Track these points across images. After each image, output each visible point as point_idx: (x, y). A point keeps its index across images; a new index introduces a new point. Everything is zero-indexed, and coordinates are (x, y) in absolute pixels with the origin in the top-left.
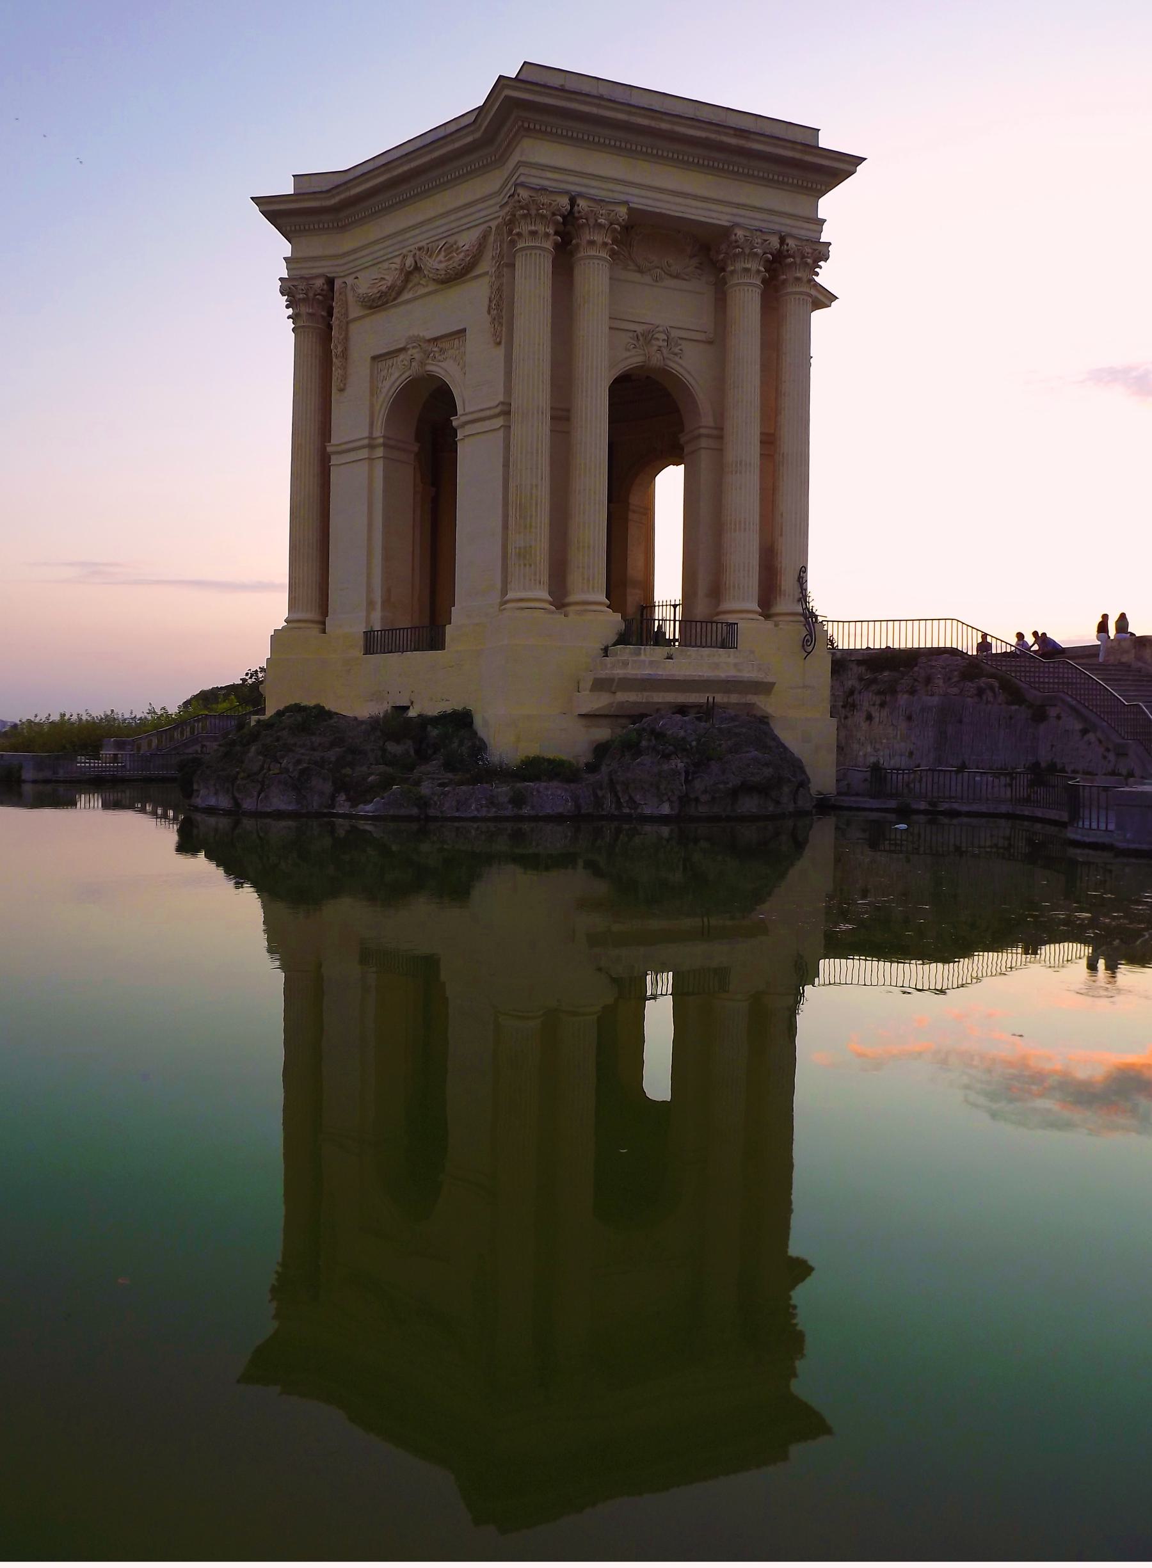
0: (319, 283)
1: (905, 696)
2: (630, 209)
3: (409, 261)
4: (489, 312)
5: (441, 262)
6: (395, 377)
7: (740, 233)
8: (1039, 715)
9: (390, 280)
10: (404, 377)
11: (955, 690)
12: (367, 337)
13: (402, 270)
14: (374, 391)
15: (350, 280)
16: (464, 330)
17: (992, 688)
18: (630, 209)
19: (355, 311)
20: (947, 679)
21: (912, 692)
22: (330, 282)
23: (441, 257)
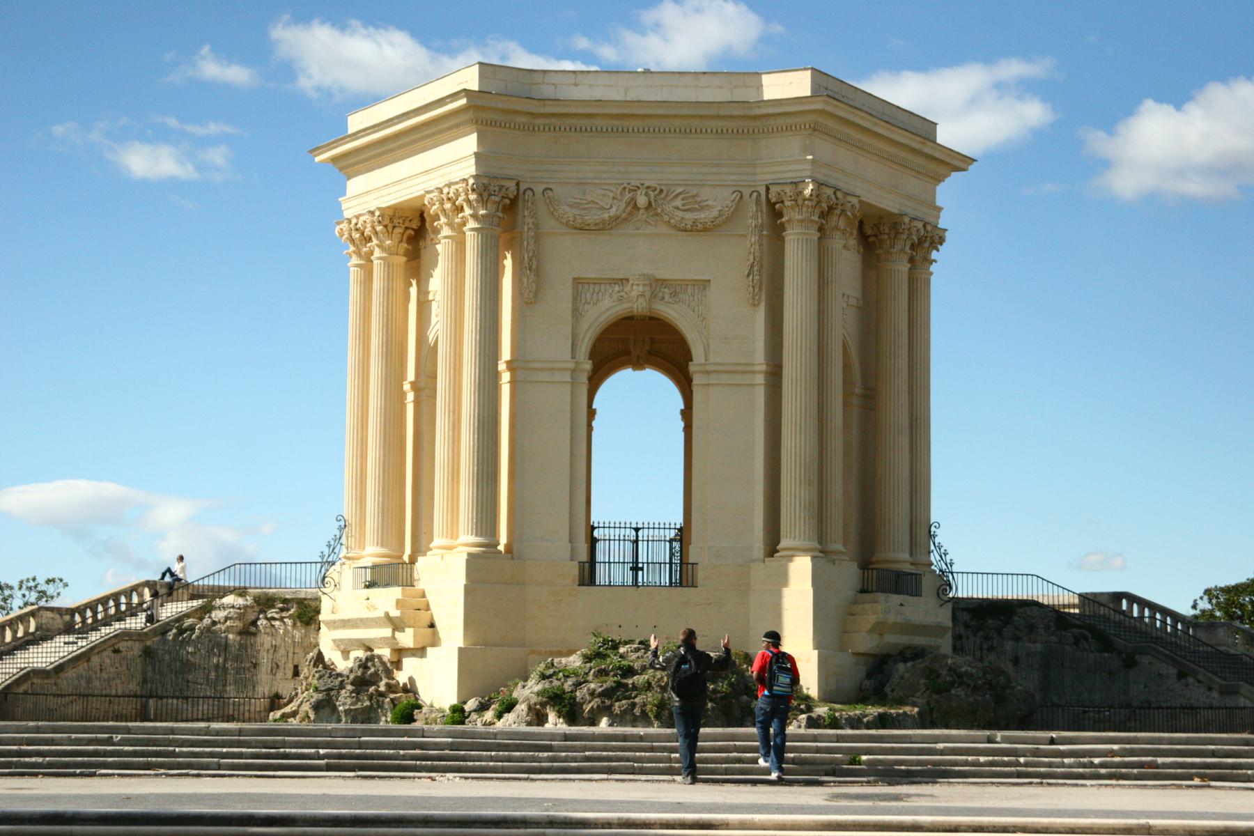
0: (511, 185)
1: (1011, 643)
2: (860, 202)
3: (642, 201)
4: (748, 275)
5: (678, 208)
6: (604, 309)
7: (907, 220)
8: (1130, 663)
9: (613, 212)
10: (619, 308)
11: (1054, 638)
12: (570, 257)
13: (628, 204)
14: (576, 313)
15: (539, 189)
17: (1086, 638)
18: (860, 202)
19: (549, 224)
20: (1047, 628)
21: (1017, 639)
22: (518, 184)
23: (678, 203)
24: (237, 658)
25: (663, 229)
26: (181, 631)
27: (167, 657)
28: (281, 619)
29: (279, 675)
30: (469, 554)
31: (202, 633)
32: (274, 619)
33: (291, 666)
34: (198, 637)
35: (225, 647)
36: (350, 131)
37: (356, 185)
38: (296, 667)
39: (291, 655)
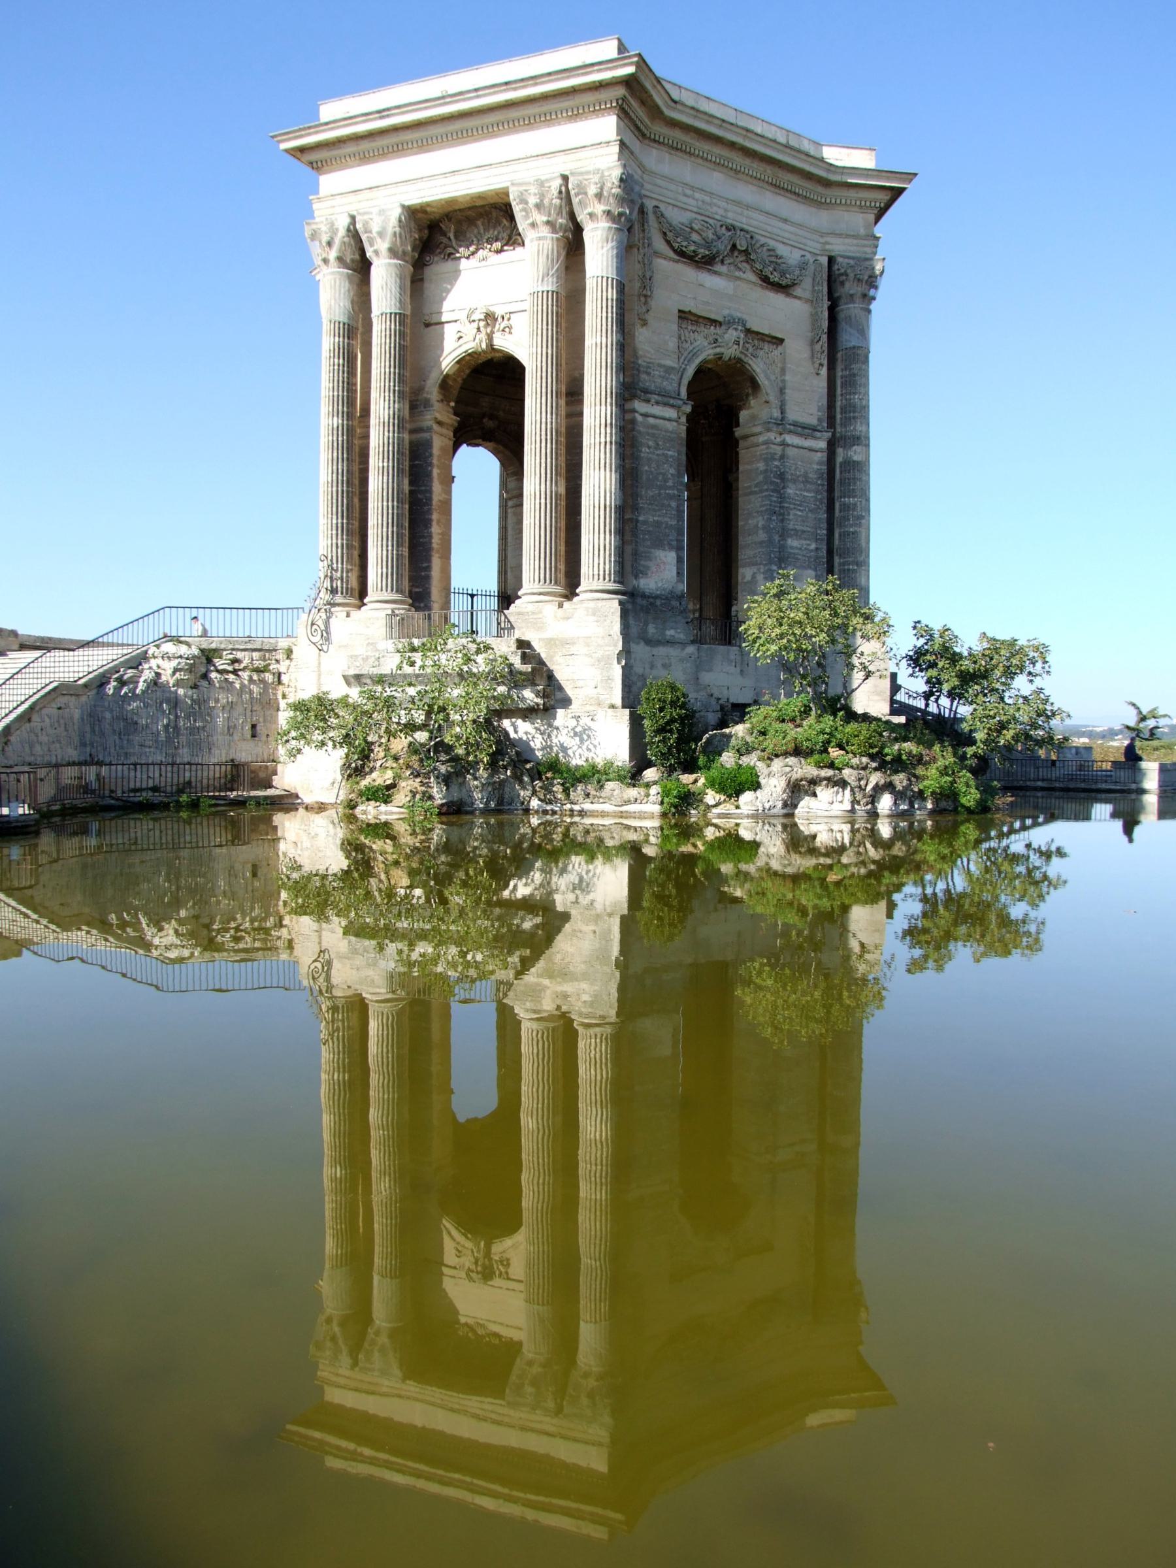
15: (649, 205)
16: (781, 341)
24: (191, 714)
25: (752, 277)
26: (122, 683)
27: (108, 715)
28: (235, 672)
29: (236, 737)
30: (621, 603)
31: (148, 687)
32: (228, 672)
33: (248, 727)
34: (143, 692)
35: (175, 702)
36: (323, 120)
37: (330, 182)
38: (254, 726)
39: (249, 713)
